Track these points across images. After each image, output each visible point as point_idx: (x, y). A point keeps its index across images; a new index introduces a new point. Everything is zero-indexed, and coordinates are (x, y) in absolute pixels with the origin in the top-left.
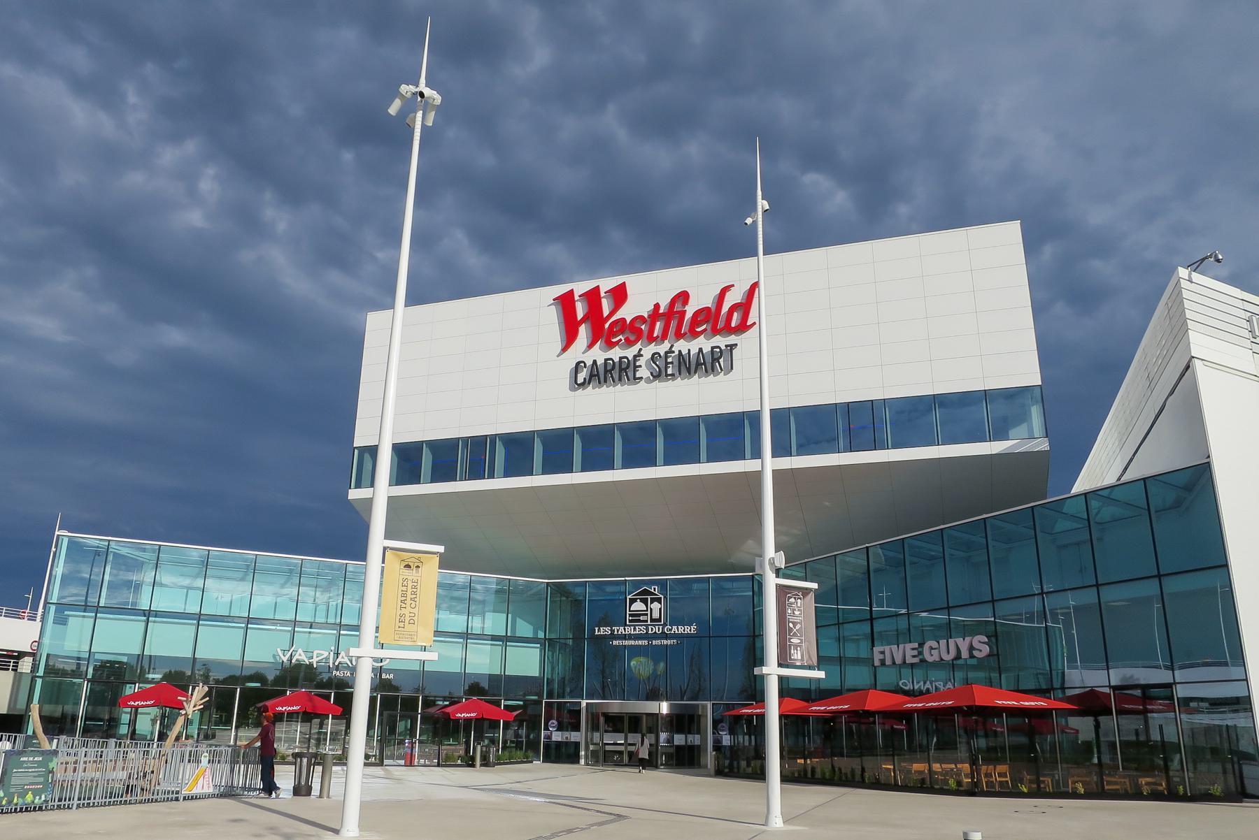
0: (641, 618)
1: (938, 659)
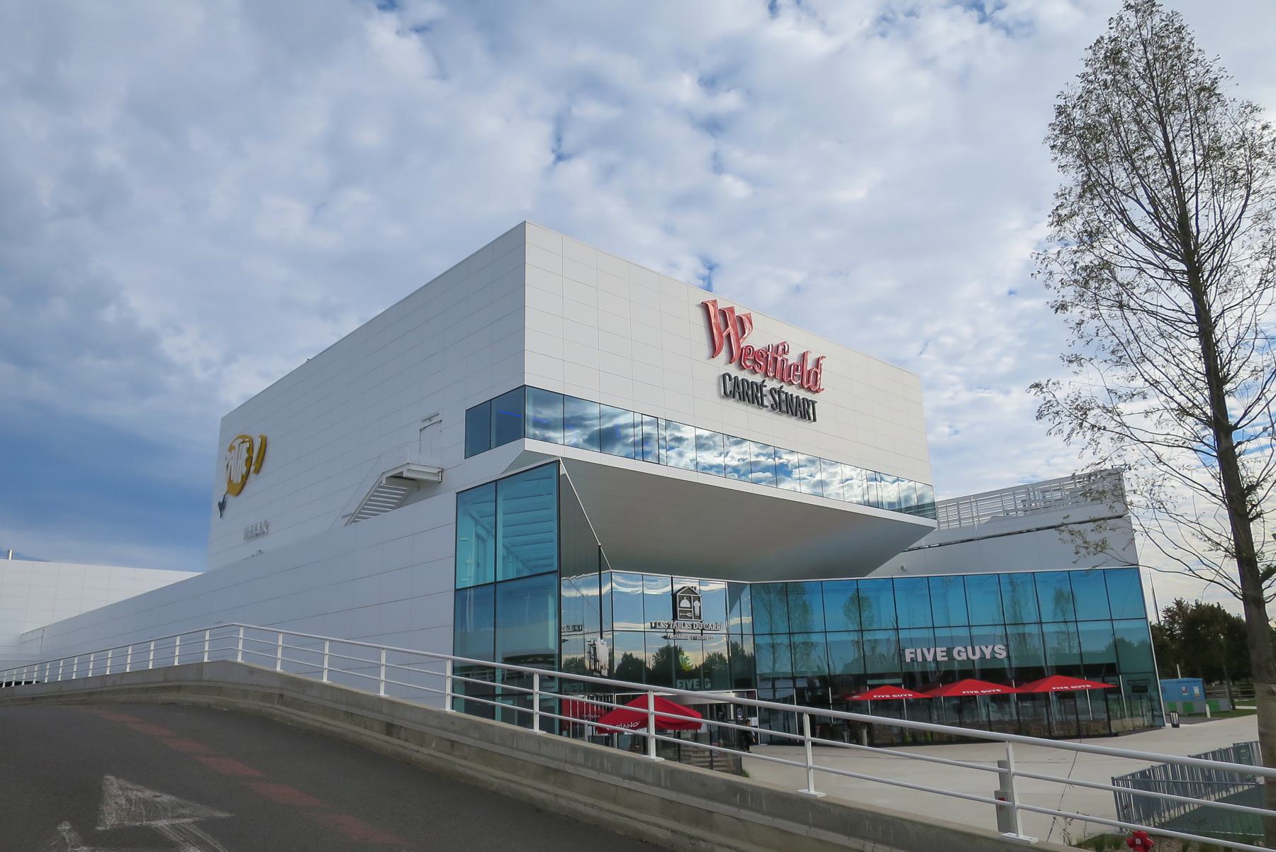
0: (688, 615)
1: (965, 659)
